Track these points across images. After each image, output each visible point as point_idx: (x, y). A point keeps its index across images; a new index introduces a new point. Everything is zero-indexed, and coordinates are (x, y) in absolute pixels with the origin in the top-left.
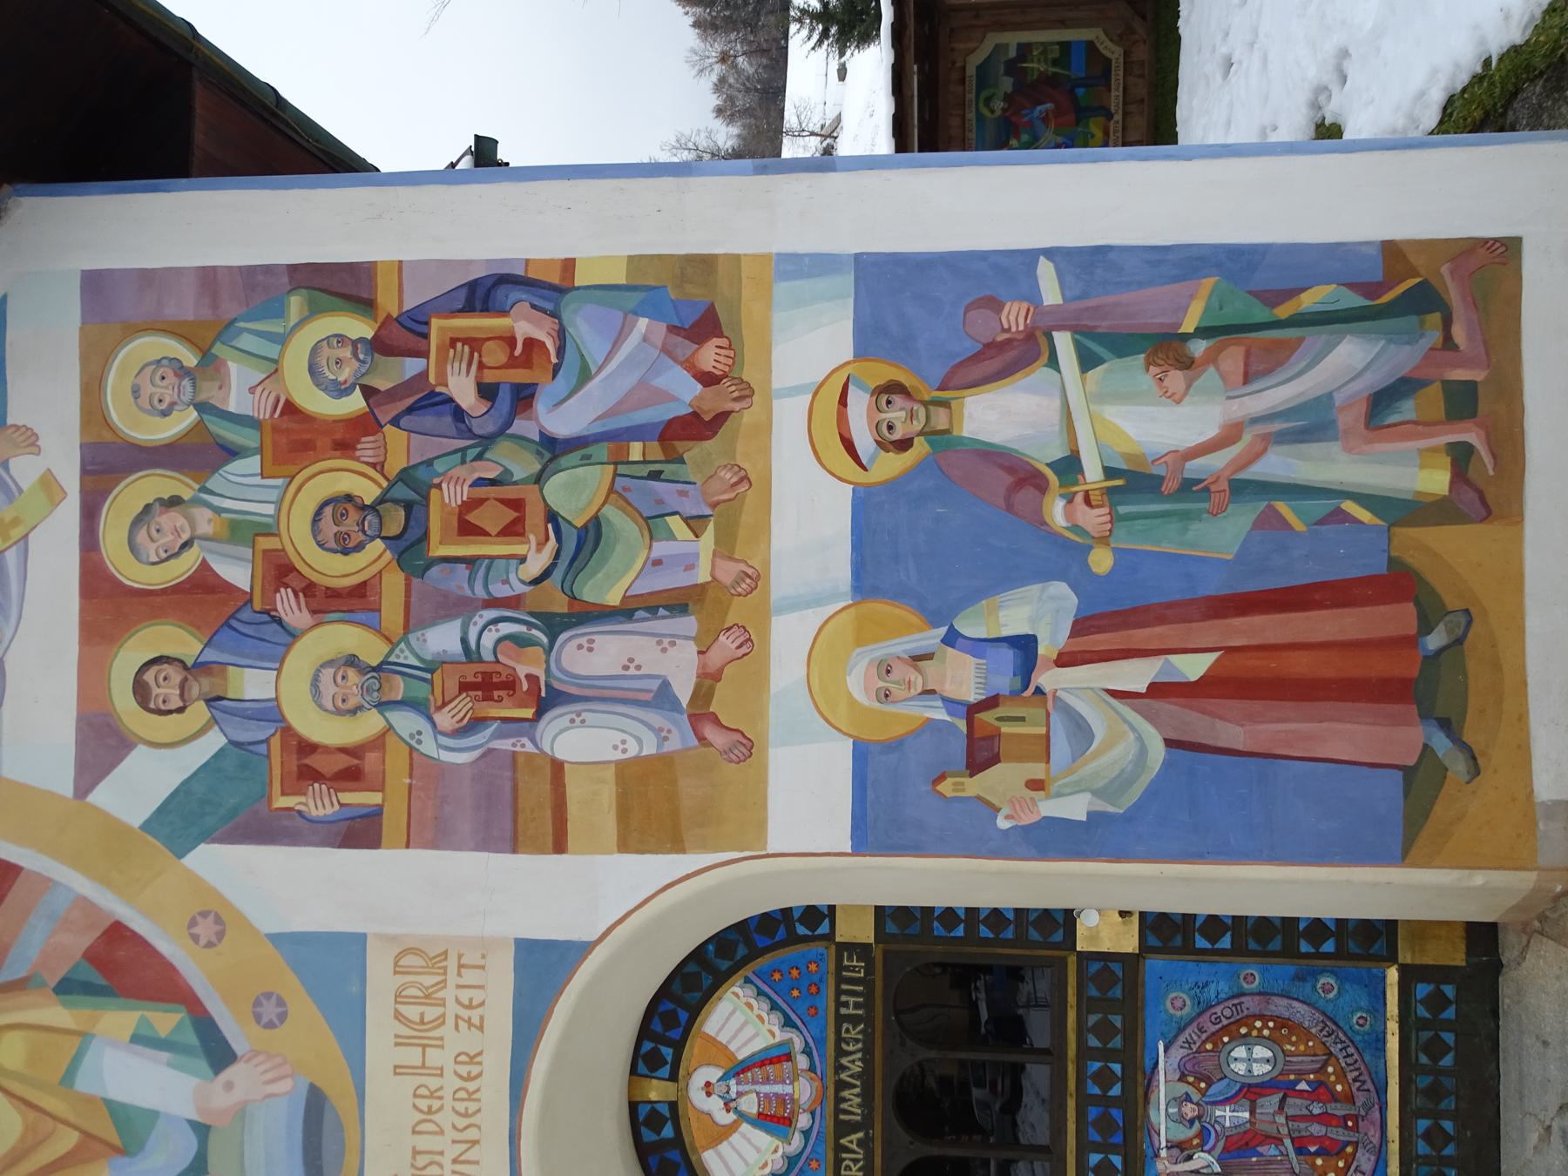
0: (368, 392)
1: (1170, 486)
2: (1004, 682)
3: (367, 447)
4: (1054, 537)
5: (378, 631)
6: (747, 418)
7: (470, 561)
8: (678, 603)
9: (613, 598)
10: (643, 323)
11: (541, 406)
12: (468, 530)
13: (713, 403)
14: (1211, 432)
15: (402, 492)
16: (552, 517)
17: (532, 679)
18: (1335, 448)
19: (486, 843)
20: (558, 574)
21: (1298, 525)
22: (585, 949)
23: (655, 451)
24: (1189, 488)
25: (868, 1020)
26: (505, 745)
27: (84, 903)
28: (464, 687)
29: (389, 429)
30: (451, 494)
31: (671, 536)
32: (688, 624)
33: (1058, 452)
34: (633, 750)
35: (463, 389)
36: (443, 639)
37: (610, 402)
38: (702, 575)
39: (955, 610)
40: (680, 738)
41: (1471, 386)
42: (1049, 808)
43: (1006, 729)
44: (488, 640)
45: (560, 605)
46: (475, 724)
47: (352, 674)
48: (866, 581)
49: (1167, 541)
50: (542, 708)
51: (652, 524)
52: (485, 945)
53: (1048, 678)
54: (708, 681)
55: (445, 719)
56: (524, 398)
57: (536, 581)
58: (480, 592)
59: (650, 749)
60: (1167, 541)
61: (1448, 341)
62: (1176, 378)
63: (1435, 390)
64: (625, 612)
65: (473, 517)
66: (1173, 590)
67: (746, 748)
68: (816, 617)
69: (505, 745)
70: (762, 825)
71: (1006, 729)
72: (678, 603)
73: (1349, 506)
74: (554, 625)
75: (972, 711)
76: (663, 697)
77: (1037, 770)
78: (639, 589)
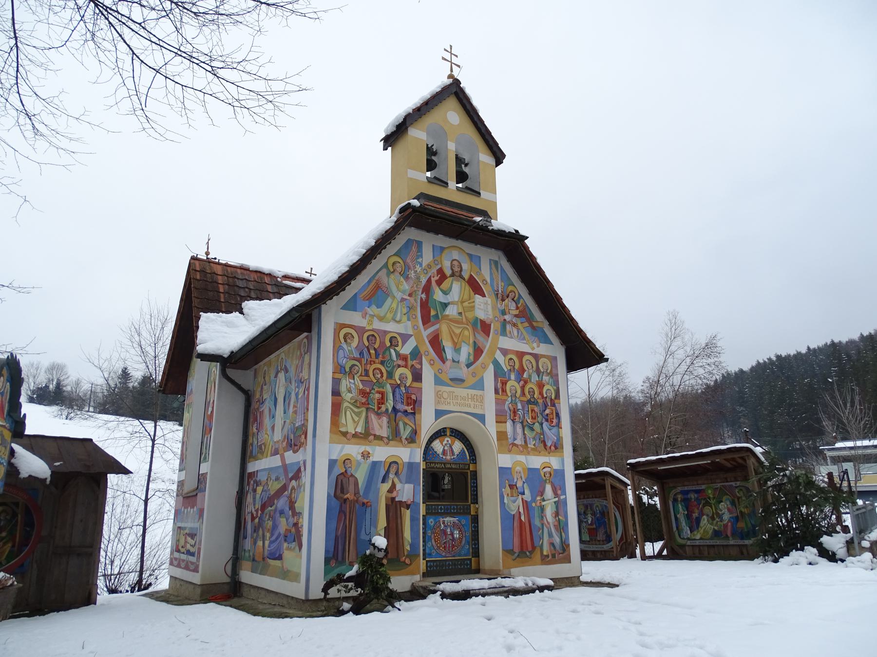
0: (546, 397)
1: (542, 514)
2: (520, 490)
3: (540, 397)
4: (536, 498)
5: (520, 397)
6: (546, 453)
7: (528, 411)
8: (526, 442)
9: (526, 432)
10: (556, 438)
11: (546, 422)
12: (532, 410)
13: (548, 448)
14: (549, 520)
15: (536, 401)
16: (534, 424)
17: (515, 419)
18: (548, 538)
19: (496, 410)
20: (527, 424)
21: (539, 533)
22: (485, 425)
23: (542, 439)
24: (542, 517)
25: (460, 469)
26: (508, 415)
27: (485, 347)
28: (514, 409)
29: (542, 400)
30: (536, 409)
31: (533, 441)
32: (523, 443)
33: (545, 498)
34: (508, 434)
35: (547, 411)
36: (519, 406)
37: (548, 434)
38: (529, 446)
39: (527, 483)
40: (510, 441)
41: (555, 557)
42: (505, 496)
43: (514, 490)
44: (520, 413)
45: (524, 424)
46: (510, 410)
47: (515, 392)
48: (530, 470)
49: (536, 514)
50: (512, 420)
51: (534, 438)
52: (484, 409)
53: (520, 496)
54: (516, 445)
55: (510, 405)
56: (547, 420)
57: (527, 421)
58: (525, 412)
59: (509, 437)
60: (536, 514)
61: (560, 554)
62: (554, 515)
63: (554, 552)
64: (524, 434)
65: (533, 412)
66: (531, 516)
67: (510, 451)
68: (525, 462)
69: (508, 415)
70: (501, 453)
71: (514, 490)
72: (526, 442)
73: (542, 540)
74: (522, 423)
75: (516, 485)
76: (515, 439)
77: (510, 495)
78: (527, 437)
